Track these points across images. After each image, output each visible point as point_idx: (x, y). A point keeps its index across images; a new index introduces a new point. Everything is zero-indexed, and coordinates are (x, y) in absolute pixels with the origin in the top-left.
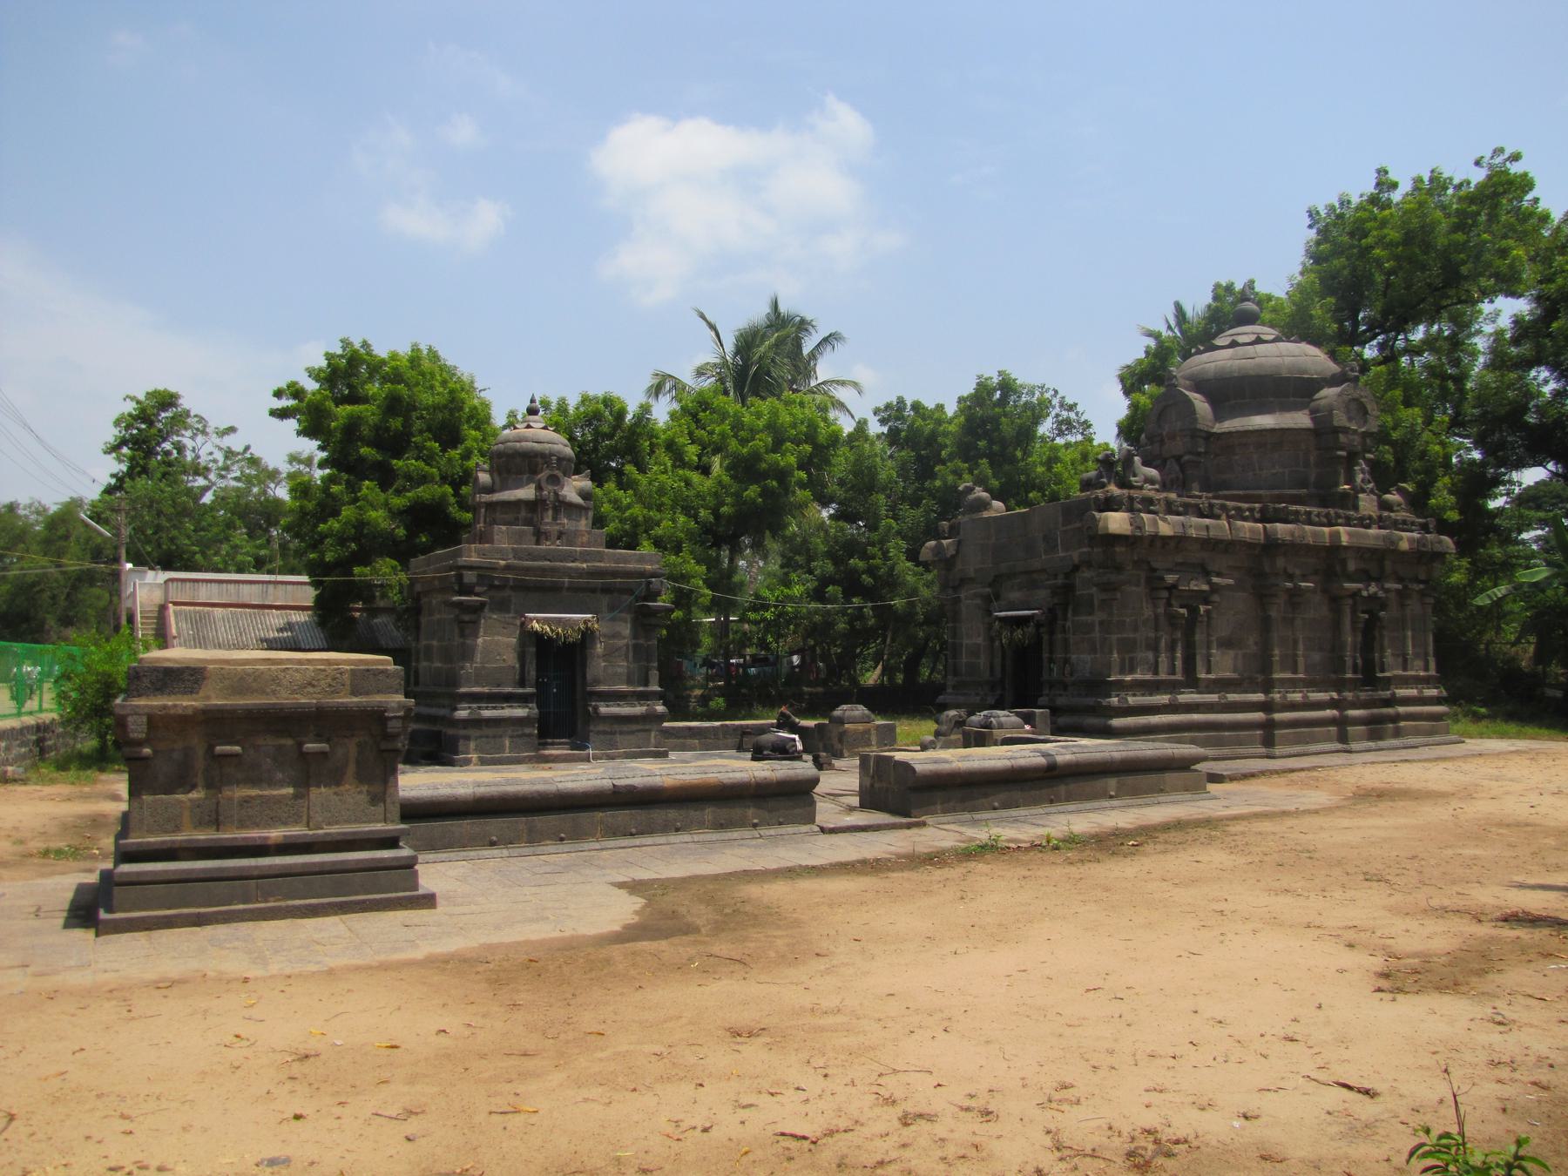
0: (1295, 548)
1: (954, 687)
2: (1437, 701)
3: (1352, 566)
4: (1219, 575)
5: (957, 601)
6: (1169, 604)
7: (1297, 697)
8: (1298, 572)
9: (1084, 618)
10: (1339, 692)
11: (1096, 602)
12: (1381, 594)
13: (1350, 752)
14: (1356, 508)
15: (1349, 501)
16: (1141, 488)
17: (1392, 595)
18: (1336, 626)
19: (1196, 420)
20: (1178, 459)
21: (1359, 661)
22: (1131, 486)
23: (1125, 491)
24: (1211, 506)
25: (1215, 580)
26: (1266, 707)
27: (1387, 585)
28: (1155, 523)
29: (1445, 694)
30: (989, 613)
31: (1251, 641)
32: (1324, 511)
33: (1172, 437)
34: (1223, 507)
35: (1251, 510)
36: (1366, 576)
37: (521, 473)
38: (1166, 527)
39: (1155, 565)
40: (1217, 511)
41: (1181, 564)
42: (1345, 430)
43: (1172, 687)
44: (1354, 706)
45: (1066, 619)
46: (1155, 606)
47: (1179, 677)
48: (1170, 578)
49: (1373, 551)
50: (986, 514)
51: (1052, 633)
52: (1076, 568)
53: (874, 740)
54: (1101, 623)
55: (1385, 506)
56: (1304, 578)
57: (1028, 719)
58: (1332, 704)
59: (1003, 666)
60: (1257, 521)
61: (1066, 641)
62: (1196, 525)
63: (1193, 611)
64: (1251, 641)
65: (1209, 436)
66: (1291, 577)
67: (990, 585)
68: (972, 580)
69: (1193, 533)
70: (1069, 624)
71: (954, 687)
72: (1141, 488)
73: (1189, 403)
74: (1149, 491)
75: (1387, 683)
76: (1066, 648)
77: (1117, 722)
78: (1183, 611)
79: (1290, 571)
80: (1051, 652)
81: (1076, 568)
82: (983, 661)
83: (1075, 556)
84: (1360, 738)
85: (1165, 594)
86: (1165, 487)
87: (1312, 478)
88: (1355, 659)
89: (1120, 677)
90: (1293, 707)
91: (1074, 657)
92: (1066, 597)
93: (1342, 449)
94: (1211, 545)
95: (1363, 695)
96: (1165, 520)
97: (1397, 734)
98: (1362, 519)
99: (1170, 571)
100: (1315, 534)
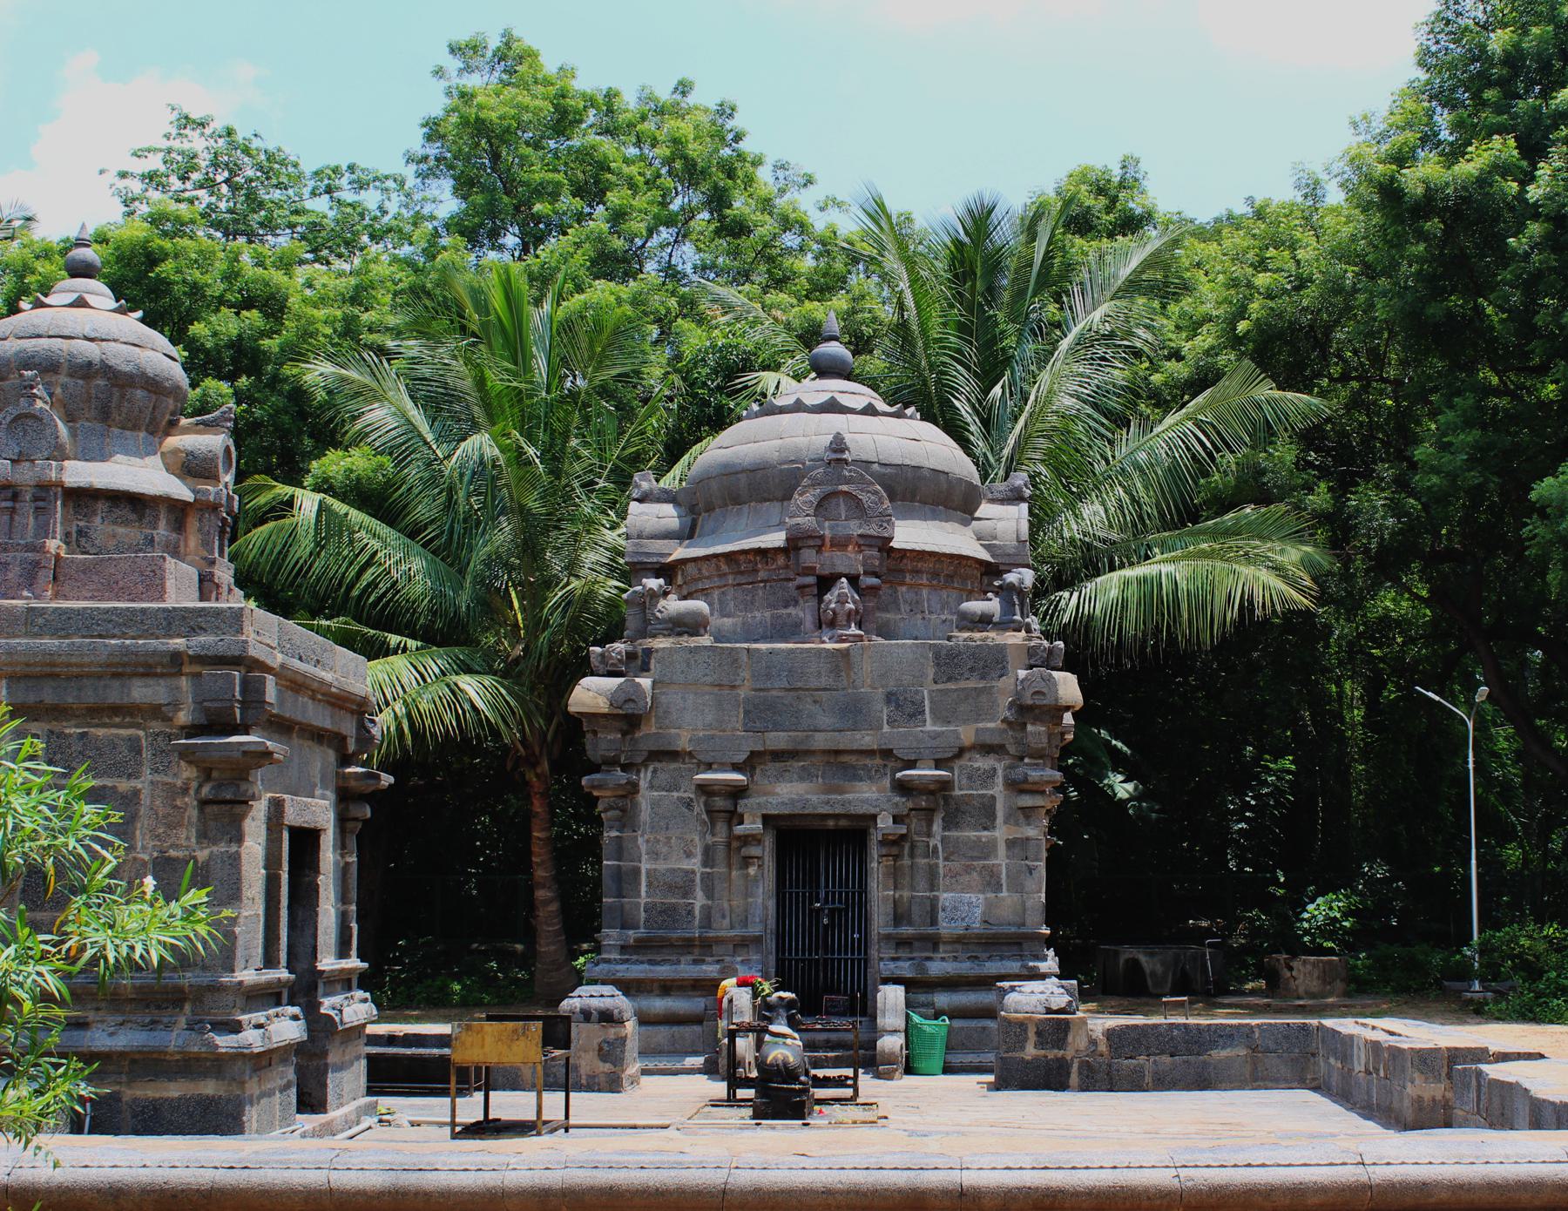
1: (624, 949)
5: (633, 788)
9: (973, 834)
33: (840, 544)
37: (132, 425)
45: (929, 835)
54: (1011, 844)
67: (736, 768)
68: (674, 755)
70: (935, 841)
71: (624, 949)
76: (933, 887)
81: (961, 752)
83: (967, 734)
91: (945, 897)
92: (933, 801)
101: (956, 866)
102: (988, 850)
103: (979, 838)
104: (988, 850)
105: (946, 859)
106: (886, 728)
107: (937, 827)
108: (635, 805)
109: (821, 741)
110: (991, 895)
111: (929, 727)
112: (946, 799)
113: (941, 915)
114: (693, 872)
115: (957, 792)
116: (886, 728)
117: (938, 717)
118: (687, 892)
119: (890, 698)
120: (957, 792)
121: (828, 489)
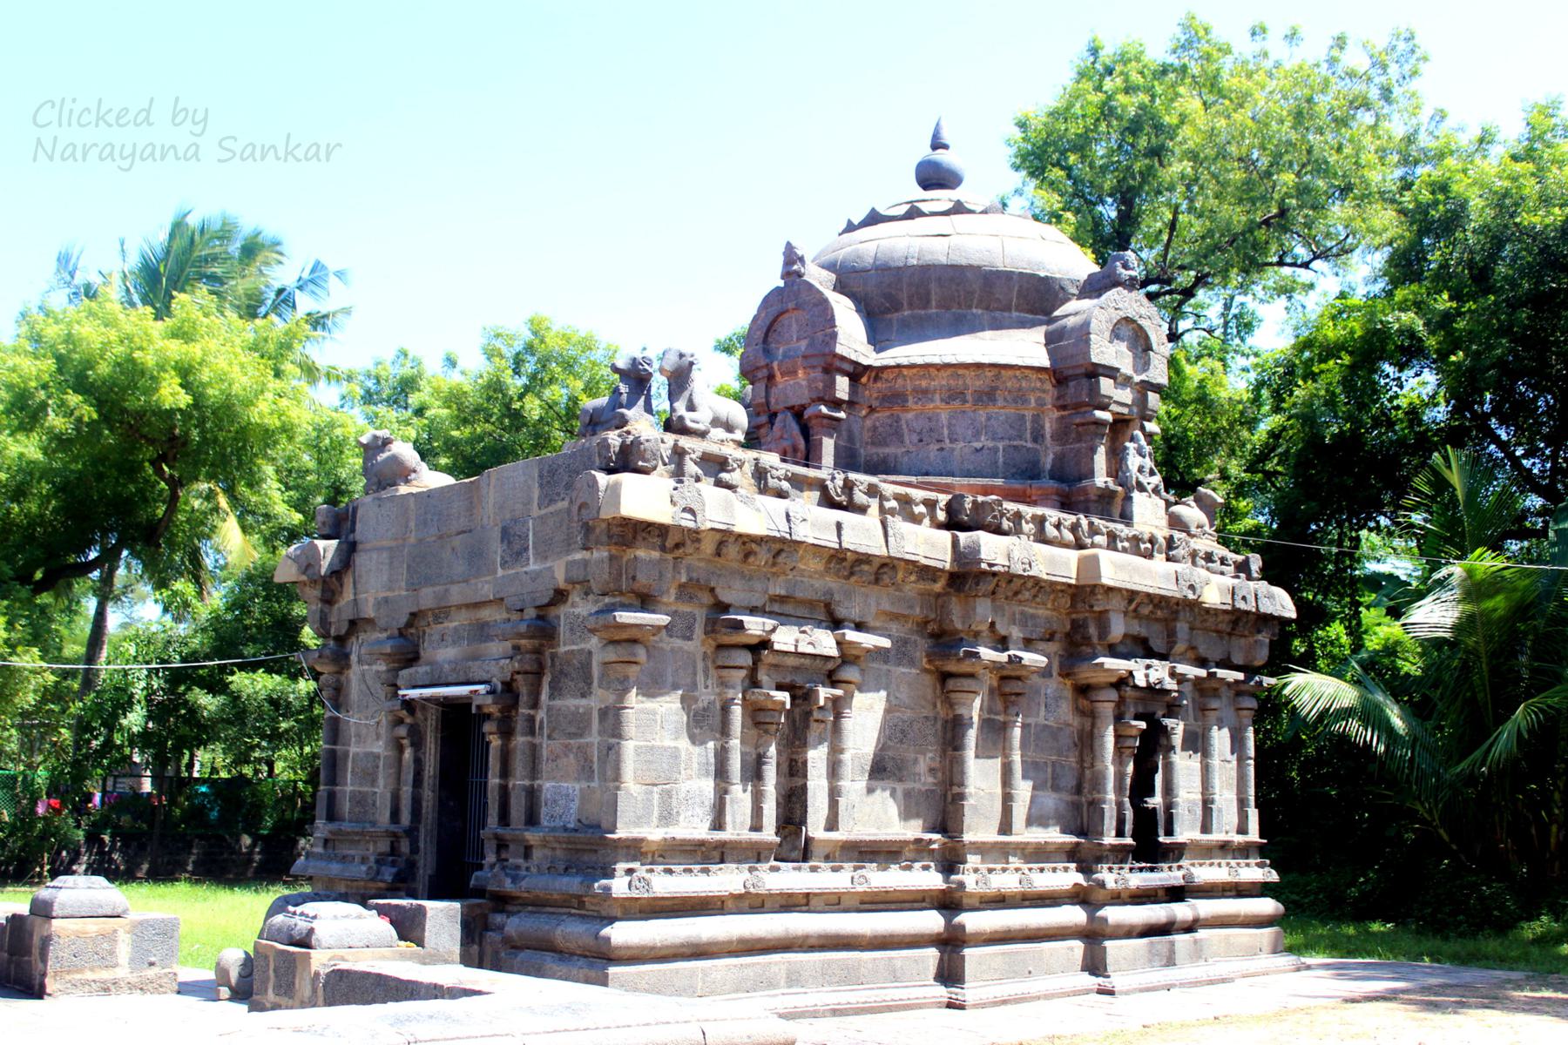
0: (1014, 586)
2: (1263, 890)
3: (1118, 628)
4: (859, 627)
6: (754, 683)
7: (1006, 881)
8: (1016, 633)
10: (1086, 869)
11: (596, 671)
12: (1170, 684)
13: (1111, 993)
14: (1126, 518)
15: (1113, 505)
16: (702, 435)
17: (1187, 688)
18: (1087, 743)
19: (834, 336)
20: (798, 413)
21: (1129, 814)
22: (684, 431)
23: (670, 438)
24: (849, 487)
25: (851, 635)
26: (949, 903)
27: (1182, 668)
28: (728, 507)
29: (1274, 876)
30: (396, 695)
31: (924, 764)
32: (1070, 519)
34: (872, 491)
35: (931, 505)
36: (1143, 648)
38: (754, 515)
39: (725, 596)
40: (860, 497)
41: (782, 599)
42: (1112, 372)
43: (753, 854)
44: (1118, 899)
45: (535, 705)
46: (723, 684)
47: (769, 834)
48: (755, 626)
49: (1157, 601)
50: (403, 490)
51: (507, 733)
52: (560, 596)
53: (124, 951)
54: (604, 713)
55: (1176, 522)
56: (1028, 644)
57: (409, 928)
58: (1078, 897)
59: (416, 802)
60: (941, 526)
61: (534, 750)
62: (812, 523)
63: (802, 696)
64: (922, 766)
65: (857, 373)
66: (1002, 643)
68: (370, 621)
69: (803, 533)
70: (541, 715)
72: (702, 435)
73: (824, 302)
74: (721, 443)
75: (1174, 853)
76: (534, 772)
77: (622, 933)
78: (784, 697)
79: (1002, 629)
80: (505, 773)
81: (560, 596)
82: (382, 789)
84: (1132, 964)
85: (745, 659)
86: (753, 440)
87: (1048, 461)
88: (1120, 805)
89: (636, 833)
90: (1000, 901)
91: (547, 786)
93: (1104, 408)
94: (845, 562)
95: (1139, 880)
96: (746, 501)
97: (1198, 953)
98: (1136, 540)
99: (753, 611)
100: (1052, 561)
101: (557, 745)
102: (580, 724)
103: (577, 707)
104: (580, 724)
105: (549, 737)
106: (500, 572)
107: (544, 696)
108: (348, 681)
109: (457, 594)
110: (584, 785)
111: (533, 566)
112: (553, 656)
113: (544, 810)
114: (377, 757)
115: (562, 649)
116: (500, 572)
117: (542, 556)
118: (374, 782)
119: (506, 534)
120: (562, 649)
121: (774, 310)
